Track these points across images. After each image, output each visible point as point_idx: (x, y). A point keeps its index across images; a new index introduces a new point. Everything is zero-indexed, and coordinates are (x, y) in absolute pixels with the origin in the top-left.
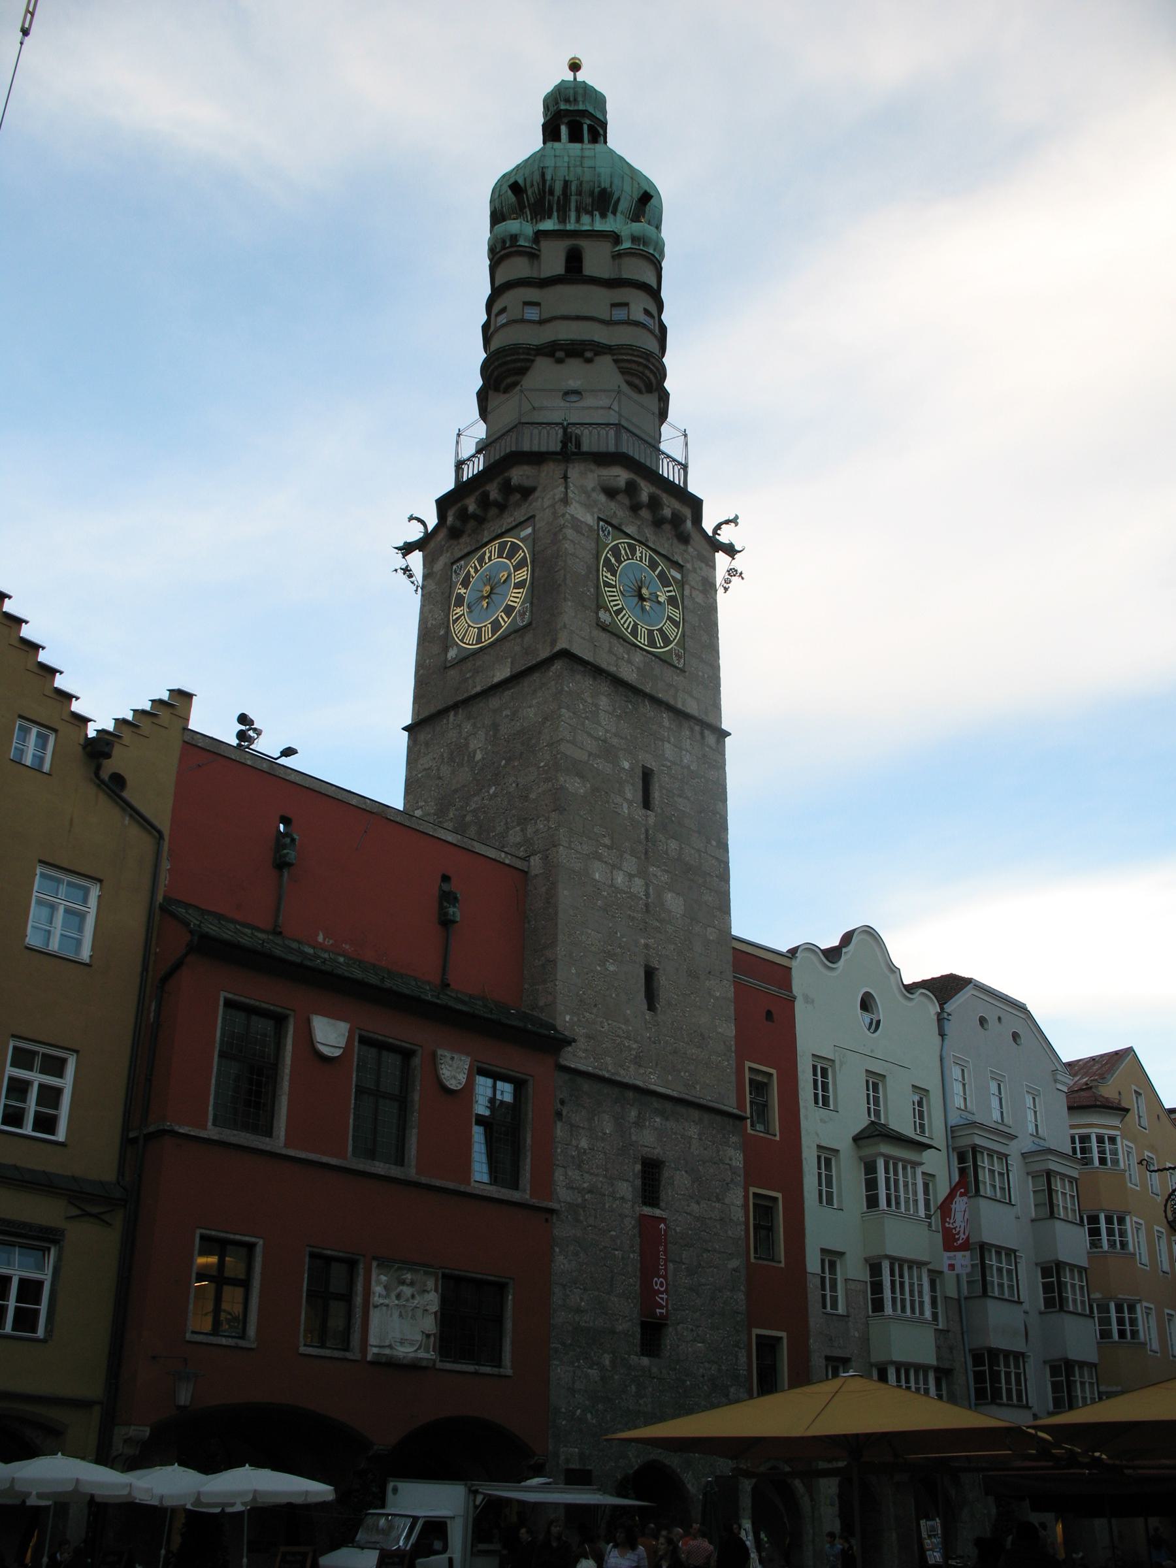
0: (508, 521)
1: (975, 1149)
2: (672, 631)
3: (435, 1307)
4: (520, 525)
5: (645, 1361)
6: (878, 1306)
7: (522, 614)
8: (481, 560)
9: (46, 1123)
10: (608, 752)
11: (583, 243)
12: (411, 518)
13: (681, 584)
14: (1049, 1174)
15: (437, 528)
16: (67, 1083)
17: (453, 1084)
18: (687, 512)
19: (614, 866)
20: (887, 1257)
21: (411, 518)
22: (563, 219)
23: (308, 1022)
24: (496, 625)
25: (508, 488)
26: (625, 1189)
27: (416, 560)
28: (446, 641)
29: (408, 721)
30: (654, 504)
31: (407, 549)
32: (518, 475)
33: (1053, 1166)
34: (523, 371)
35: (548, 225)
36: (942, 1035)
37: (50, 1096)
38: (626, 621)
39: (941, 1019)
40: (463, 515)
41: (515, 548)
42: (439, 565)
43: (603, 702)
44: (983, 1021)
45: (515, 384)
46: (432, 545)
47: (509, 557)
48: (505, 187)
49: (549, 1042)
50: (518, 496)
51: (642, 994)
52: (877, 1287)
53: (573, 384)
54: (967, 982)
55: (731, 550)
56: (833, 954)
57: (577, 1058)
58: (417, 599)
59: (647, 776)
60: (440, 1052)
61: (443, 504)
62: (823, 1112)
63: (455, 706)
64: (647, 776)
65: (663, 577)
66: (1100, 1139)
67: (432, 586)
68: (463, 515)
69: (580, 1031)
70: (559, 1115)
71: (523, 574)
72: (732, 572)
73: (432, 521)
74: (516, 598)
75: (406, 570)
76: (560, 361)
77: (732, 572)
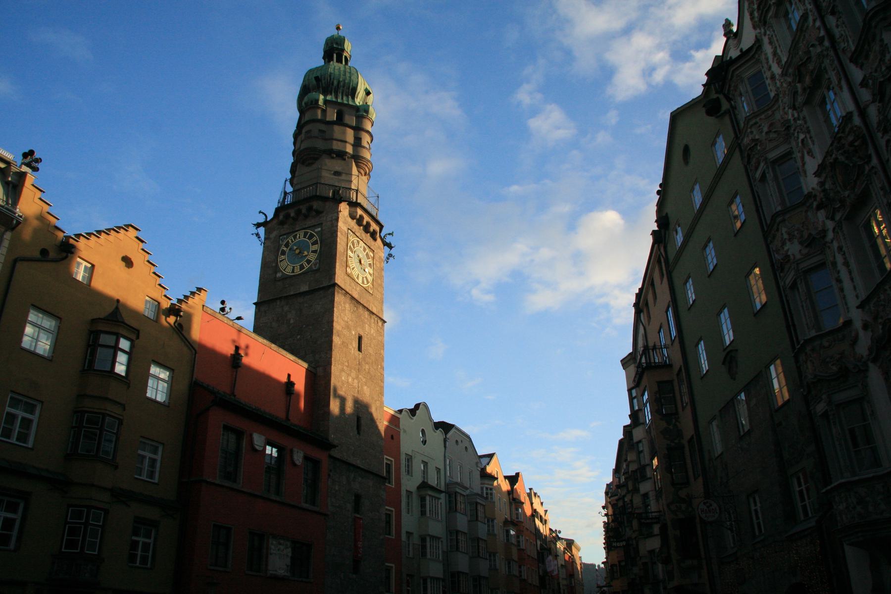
0: (309, 222)
1: (456, 493)
2: (370, 278)
3: (290, 554)
4: (315, 226)
5: (354, 576)
6: (424, 554)
7: (315, 265)
8: (295, 237)
9: (151, 474)
10: (348, 327)
11: (345, 109)
12: (260, 212)
13: (373, 258)
14: (477, 503)
15: (272, 220)
16: (158, 457)
17: (297, 463)
18: (378, 229)
19: (348, 375)
20: (429, 535)
21: (260, 212)
22: (337, 98)
23: (251, 435)
24: (302, 267)
25: (310, 209)
26: (350, 506)
27: (262, 231)
28: (276, 269)
29: (256, 301)
30: (368, 224)
31: (258, 225)
32: (316, 205)
33: (478, 501)
34: (317, 159)
35: (329, 98)
36: (445, 447)
37: (153, 462)
38: (355, 273)
39: (445, 441)
40: (287, 216)
41: (312, 236)
42: (273, 236)
43: (347, 306)
44: (457, 441)
45: (312, 164)
46: (270, 225)
47: (310, 238)
48: (312, 77)
49: (326, 445)
50: (314, 213)
51: (355, 428)
52: (424, 547)
53: (338, 169)
54: (452, 426)
55: (389, 246)
56: (413, 412)
57: (335, 453)
58: (260, 249)
59: (360, 338)
60: (295, 450)
61: (278, 211)
62: (408, 477)
63: (280, 298)
64: (360, 338)
65: (367, 254)
66: (487, 488)
67: (268, 243)
68: (287, 216)
69: (336, 442)
70: (329, 475)
71: (316, 247)
72: (390, 255)
73: (270, 216)
74: (313, 257)
75: (257, 235)
76: (333, 158)
77: (390, 255)
